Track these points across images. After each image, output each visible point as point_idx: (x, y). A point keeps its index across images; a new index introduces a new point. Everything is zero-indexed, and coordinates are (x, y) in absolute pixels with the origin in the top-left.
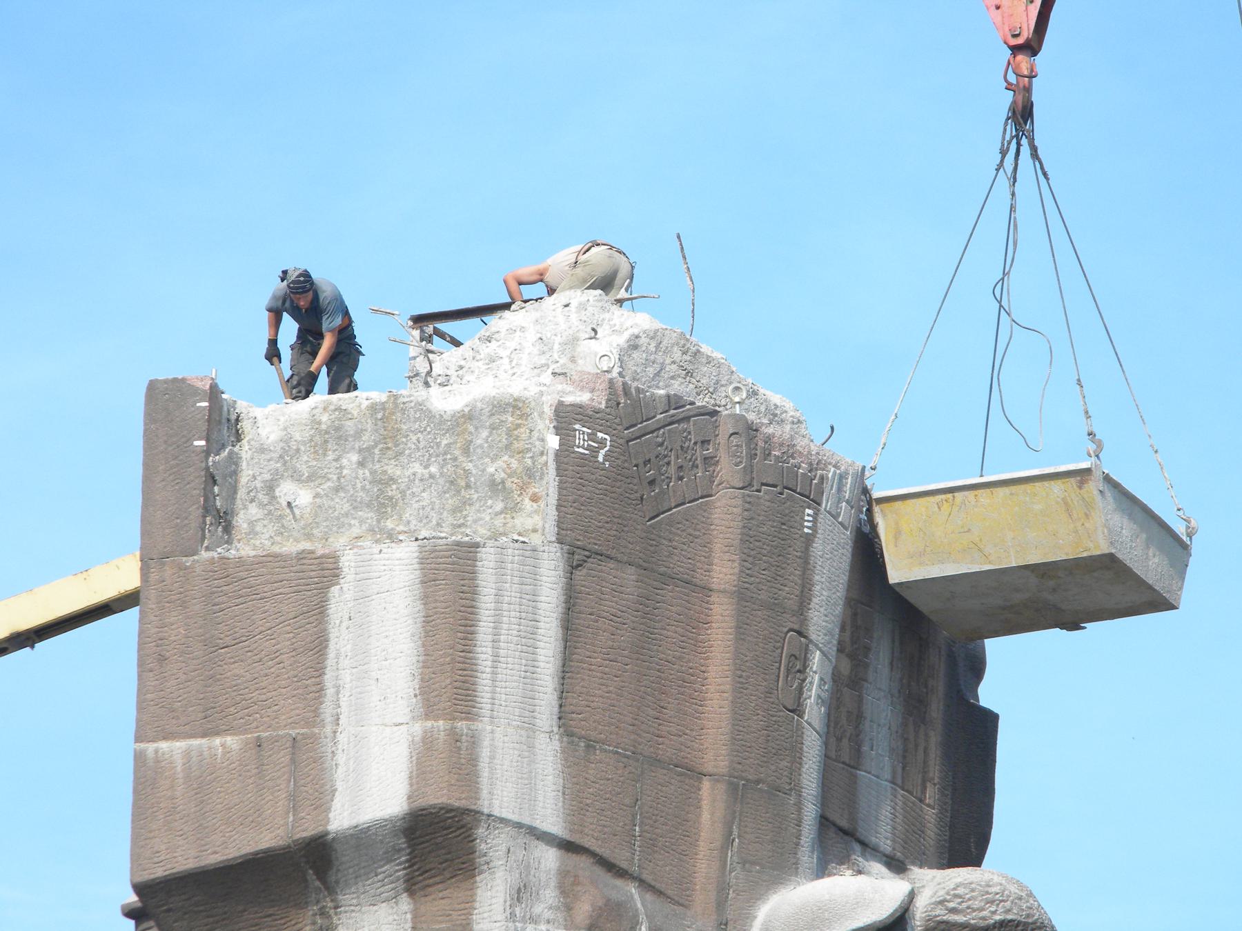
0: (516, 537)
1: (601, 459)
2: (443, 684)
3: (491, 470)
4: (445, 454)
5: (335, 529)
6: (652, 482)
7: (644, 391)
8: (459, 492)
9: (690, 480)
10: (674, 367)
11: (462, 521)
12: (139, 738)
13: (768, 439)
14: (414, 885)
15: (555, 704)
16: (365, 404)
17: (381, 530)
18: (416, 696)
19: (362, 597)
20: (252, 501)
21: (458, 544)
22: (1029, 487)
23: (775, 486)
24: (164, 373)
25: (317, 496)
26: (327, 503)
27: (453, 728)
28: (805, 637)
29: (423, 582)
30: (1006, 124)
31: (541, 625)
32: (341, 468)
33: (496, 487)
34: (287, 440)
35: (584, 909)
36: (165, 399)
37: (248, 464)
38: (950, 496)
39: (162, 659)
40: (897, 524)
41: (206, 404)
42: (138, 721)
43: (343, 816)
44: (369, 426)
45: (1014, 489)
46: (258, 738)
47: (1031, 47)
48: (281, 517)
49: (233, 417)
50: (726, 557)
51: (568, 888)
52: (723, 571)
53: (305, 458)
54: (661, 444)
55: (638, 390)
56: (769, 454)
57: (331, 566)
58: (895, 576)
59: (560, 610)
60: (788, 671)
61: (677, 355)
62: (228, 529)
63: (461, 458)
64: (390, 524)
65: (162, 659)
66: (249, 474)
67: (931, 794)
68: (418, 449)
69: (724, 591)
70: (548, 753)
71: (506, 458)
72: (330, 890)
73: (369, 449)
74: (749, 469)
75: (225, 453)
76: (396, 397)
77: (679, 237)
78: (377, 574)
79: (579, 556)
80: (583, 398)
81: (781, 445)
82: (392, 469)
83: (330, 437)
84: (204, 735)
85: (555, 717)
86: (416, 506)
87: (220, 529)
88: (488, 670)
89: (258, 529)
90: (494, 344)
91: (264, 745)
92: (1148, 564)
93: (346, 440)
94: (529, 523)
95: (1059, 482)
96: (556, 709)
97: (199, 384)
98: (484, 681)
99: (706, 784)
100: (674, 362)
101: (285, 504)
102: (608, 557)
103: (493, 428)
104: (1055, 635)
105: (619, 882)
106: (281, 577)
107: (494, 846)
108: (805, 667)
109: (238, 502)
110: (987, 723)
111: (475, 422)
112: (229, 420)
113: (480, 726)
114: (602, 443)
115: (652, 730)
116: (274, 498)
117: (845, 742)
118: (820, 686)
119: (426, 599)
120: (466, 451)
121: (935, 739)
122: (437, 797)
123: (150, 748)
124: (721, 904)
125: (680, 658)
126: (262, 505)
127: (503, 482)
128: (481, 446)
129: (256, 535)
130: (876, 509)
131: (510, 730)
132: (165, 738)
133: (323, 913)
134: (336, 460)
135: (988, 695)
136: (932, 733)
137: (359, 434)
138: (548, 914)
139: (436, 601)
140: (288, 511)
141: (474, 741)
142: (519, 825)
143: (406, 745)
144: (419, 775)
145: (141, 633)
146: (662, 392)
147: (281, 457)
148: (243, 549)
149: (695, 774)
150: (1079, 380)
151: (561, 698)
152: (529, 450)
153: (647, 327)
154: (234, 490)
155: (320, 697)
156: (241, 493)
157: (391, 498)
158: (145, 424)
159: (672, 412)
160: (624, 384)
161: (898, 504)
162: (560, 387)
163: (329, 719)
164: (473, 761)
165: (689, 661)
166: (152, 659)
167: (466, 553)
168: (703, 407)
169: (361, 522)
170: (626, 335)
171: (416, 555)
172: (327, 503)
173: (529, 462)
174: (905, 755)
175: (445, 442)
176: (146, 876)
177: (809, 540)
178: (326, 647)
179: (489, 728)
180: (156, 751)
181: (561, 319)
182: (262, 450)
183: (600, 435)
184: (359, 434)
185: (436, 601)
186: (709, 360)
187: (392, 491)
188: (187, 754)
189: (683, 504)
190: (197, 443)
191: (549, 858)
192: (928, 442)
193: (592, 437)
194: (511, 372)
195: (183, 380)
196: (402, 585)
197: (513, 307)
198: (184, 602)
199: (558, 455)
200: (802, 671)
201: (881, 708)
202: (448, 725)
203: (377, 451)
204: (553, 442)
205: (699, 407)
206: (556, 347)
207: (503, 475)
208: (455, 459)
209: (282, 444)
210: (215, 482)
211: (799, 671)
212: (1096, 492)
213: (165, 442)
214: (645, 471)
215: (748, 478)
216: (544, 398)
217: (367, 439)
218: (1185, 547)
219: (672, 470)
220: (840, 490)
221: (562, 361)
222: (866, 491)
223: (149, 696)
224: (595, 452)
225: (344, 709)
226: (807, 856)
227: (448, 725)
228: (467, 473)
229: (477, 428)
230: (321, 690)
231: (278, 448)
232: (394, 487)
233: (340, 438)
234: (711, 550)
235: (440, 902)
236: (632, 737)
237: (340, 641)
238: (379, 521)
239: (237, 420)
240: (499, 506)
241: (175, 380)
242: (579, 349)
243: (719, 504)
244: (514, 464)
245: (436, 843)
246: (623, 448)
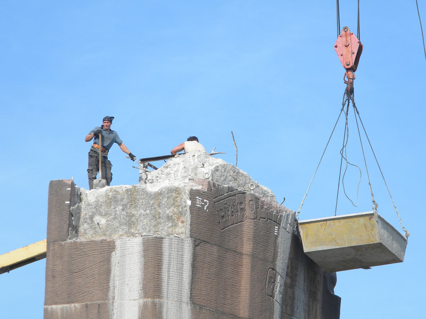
0: (176, 235)
1: (205, 209)
2: (150, 286)
3: (168, 212)
4: (152, 206)
5: (114, 232)
6: (223, 217)
7: (220, 186)
8: (156, 220)
9: (236, 216)
10: (230, 177)
11: (157, 230)
12: (45, 304)
13: (263, 202)
15: (189, 293)
16: (124, 189)
17: (129, 233)
18: (141, 290)
19: (123, 256)
20: (85, 222)
21: (156, 237)
22: (352, 220)
23: (265, 218)
25: (107, 221)
26: (111, 223)
27: (154, 301)
28: (275, 271)
29: (144, 251)
30: (344, 95)
31: (184, 265)
32: (116, 211)
33: (169, 218)
34: (97, 201)
36: (56, 187)
37: (84, 210)
38: (325, 222)
39: (54, 277)
40: (307, 232)
41: (70, 189)
42: (45, 298)
44: (126, 197)
45: (347, 220)
46: (87, 304)
47: (353, 69)
48: (95, 228)
49: (79, 194)
50: (248, 242)
52: (247, 247)
53: (104, 208)
54: (226, 204)
55: (218, 185)
56: (263, 207)
57: (112, 245)
58: (306, 249)
59: (191, 261)
60: (269, 282)
61: (231, 173)
62: (77, 232)
63: (157, 208)
64: (132, 231)
65: (54, 277)
66: (85, 212)
68: (143, 205)
69: (247, 255)
71: (173, 208)
74: (256, 213)
75: (76, 206)
76: (135, 187)
77: (232, 133)
78: (128, 248)
79: (197, 242)
80: (199, 187)
81: (267, 204)
82: (134, 212)
83: (113, 200)
84: (68, 303)
85: (189, 298)
86: (141, 224)
87: (74, 232)
88: (166, 281)
89: (87, 232)
90: (169, 169)
91: (89, 307)
92: (393, 246)
93: (118, 202)
94: (180, 231)
95: (363, 218)
96: (189, 295)
97: (67, 182)
100: (230, 176)
101: (96, 223)
102: (207, 242)
103: (168, 198)
104: (361, 271)
106: (95, 249)
108: (275, 281)
109: (80, 223)
110: (338, 300)
111: (162, 196)
112: (77, 194)
113: (163, 300)
114: (206, 203)
115: (222, 302)
116: (93, 221)
117: (288, 307)
118: (280, 287)
119: (145, 256)
120: (159, 206)
121: (319, 306)
123: (49, 307)
125: (232, 278)
126: (88, 224)
127: (172, 216)
128: (164, 204)
129: (86, 234)
130: (300, 227)
131: (173, 302)
132: (55, 304)
134: (114, 208)
135: (337, 291)
136: (318, 304)
137: (122, 200)
139: (148, 257)
140: (98, 226)
141: (161, 306)
143: (137, 307)
145: (47, 268)
146: (226, 186)
147: (95, 207)
148: (82, 239)
150: (369, 183)
151: (191, 291)
152: (181, 205)
153: (221, 163)
154: (79, 218)
155: (108, 290)
156: (82, 220)
157: (133, 222)
158: (49, 196)
159: (230, 193)
160: (214, 183)
161: (307, 225)
162: (191, 184)
163: (111, 298)
164: (161, 312)
165: (235, 278)
166: (51, 276)
167: (159, 241)
168: (241, 191)
169: (123, 230)
170: (214, 166)
171: (142, 241)
172: (111, 223)
173: (181, 209)
175: (152, 202)
177: (276, 237)
178: (110, 273)
179: (166, 301)
180: (52, 308)
181: (192, 161)
182: (89, 205)
183: (205, 200)
184: (122, 200)
185: (148, 257)
186: (242, 175)
187: (133, 219)
188: (62, 309)
189: (233, 224)
190: (66, 202)
192: (318, 203)
193: (202, 201)
194: (174, 179)
195: (62, 181)
196: (137, 251)
197: (175, 156)
198: (62, 257)
199: (191, 207)
200: (274, 282)
201: (301, 296)
202: (152, 300)
203: (128, 205)
204: (189, 203)
205: (239, 191)
206: (190, 170)
207: (172, 214)
208: (155, 208)
209: (96, 203)
210: (72, 216)
211: (273, 282)
212: (375, 222)
213: (56, 202)
215: (256, 216)
216: (186, 188)
217: (125, 201)
218: (405, 241)
219: (230, 212)
220: (287, 220)
221: (192, 175)
222: (296, 220)
223: (49, 289)
224: (203, 206)
225: (116, 295)
227: (152, 300)
228: (159, 213)
229: (163, 198)
230: (108, 288)
231: (94, 204)
232: (134, 218)
233: (115, 201)
234: (243, 240)
236: (215, 304)
237: (115, 271)
238: (129, 230)
239: (80, 195)
240: (170, 225)
241: (59, 181)
242: (198, 171)
243: (245, 224)
244: (176, 210)
246: (213, 205)
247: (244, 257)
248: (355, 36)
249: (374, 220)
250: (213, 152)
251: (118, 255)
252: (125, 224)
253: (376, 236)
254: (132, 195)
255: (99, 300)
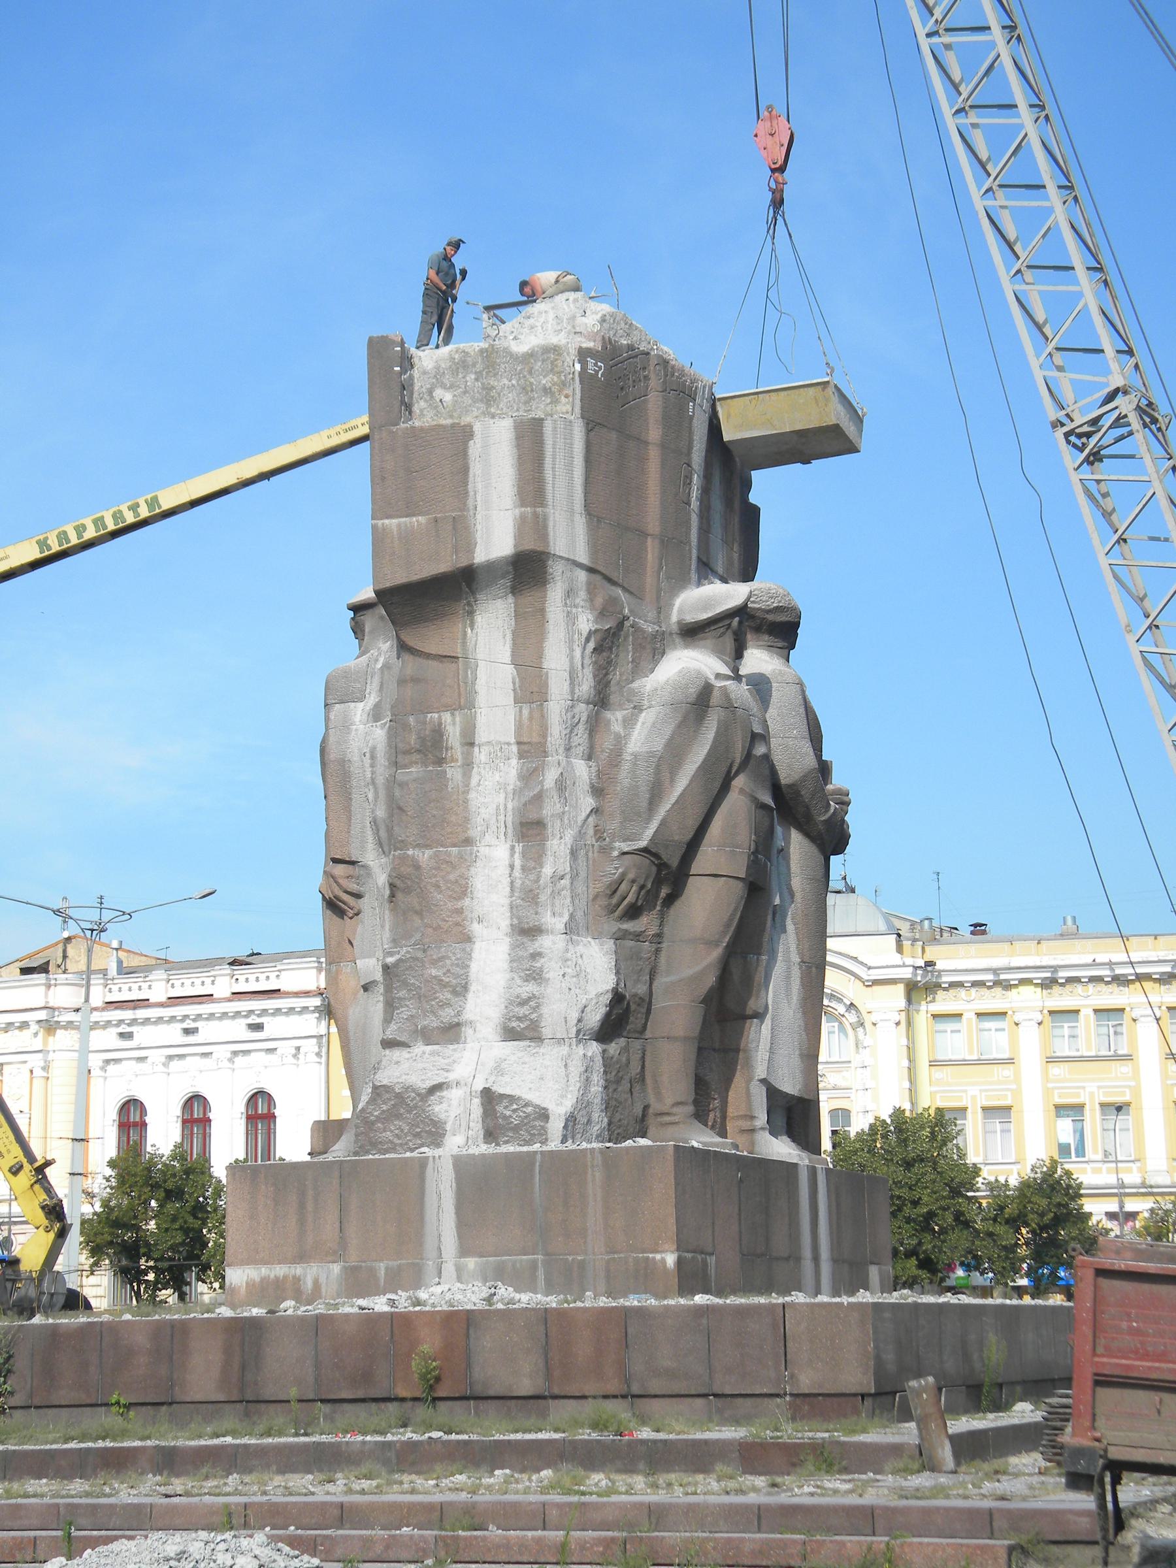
13: (673, 367)
14: (515, 590)
21: (534, 419)
24: (377, 333)
33: (546, 391)
34: (437, 368)
35: (599, 601)
43: (481, 556)
47: (782, 169)
51: (591, 590)
52: (654, 434)
58: (727, 437)
61: (623, 325)
62: (410, 413)
65: (383, 479)
67: (736, 547)
70: (580, 522)
72: (473, 593)
73: (480, 372)
74: (665, 382)
79: (591, 426)
80: (591, 345)
82: (493, 382)
83: (461, 365)
90: (532, 321)
92: (850, 429)
98: (549, 487)
99: (649, 540)
103: (543, 361)
105: (613, 588)
107: (556, 569)
114: (600, 368)
116: (432, 397)
120: (530, 372)
121: (736, 519)
122: (529, 545)
123: (380, 522)
124: (658, 598)
126: (426, 401)
129: (424, 416)
130: (718, 404)
133: (469, 604)
135: (753, 498)
137: (474, 365)
138: (582, 603)
142: (568, 560)
144: (519, 535)
148: (417, 424)
149: (644, 534)
156: (415, 395)
164: (545, 527)
166: (378, 478)
167: (538, 423)
169: (478, 409)
170: (600, 315)
174: (726, 527)
176: (381, 586)
177: (692, 418)
182: (425, 373)
188: (399, 525)
191: (582, 576)
193: (596, 365)
199: (580, 374)
201: (717, 504)
204: (578, 367)
214: (619, 381)
217: (479, 367)
224: (597, 372)
226: (694, 576)
228: (531, 384)
235: (528, 598)
237: (476, 469)
240: (549, 400)
241: (382, 337)
245: (527, 570)
246: (609, 369)
247: (650, 447)
248: (783, 119)
249: (830, 390)
250: (593, 294)
251: (478, 446)
252: (482, 401)
253: (834, 414)
254: (491, 358)
255: (453, 511)
